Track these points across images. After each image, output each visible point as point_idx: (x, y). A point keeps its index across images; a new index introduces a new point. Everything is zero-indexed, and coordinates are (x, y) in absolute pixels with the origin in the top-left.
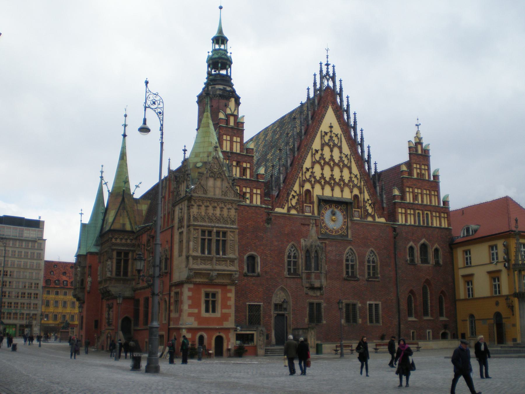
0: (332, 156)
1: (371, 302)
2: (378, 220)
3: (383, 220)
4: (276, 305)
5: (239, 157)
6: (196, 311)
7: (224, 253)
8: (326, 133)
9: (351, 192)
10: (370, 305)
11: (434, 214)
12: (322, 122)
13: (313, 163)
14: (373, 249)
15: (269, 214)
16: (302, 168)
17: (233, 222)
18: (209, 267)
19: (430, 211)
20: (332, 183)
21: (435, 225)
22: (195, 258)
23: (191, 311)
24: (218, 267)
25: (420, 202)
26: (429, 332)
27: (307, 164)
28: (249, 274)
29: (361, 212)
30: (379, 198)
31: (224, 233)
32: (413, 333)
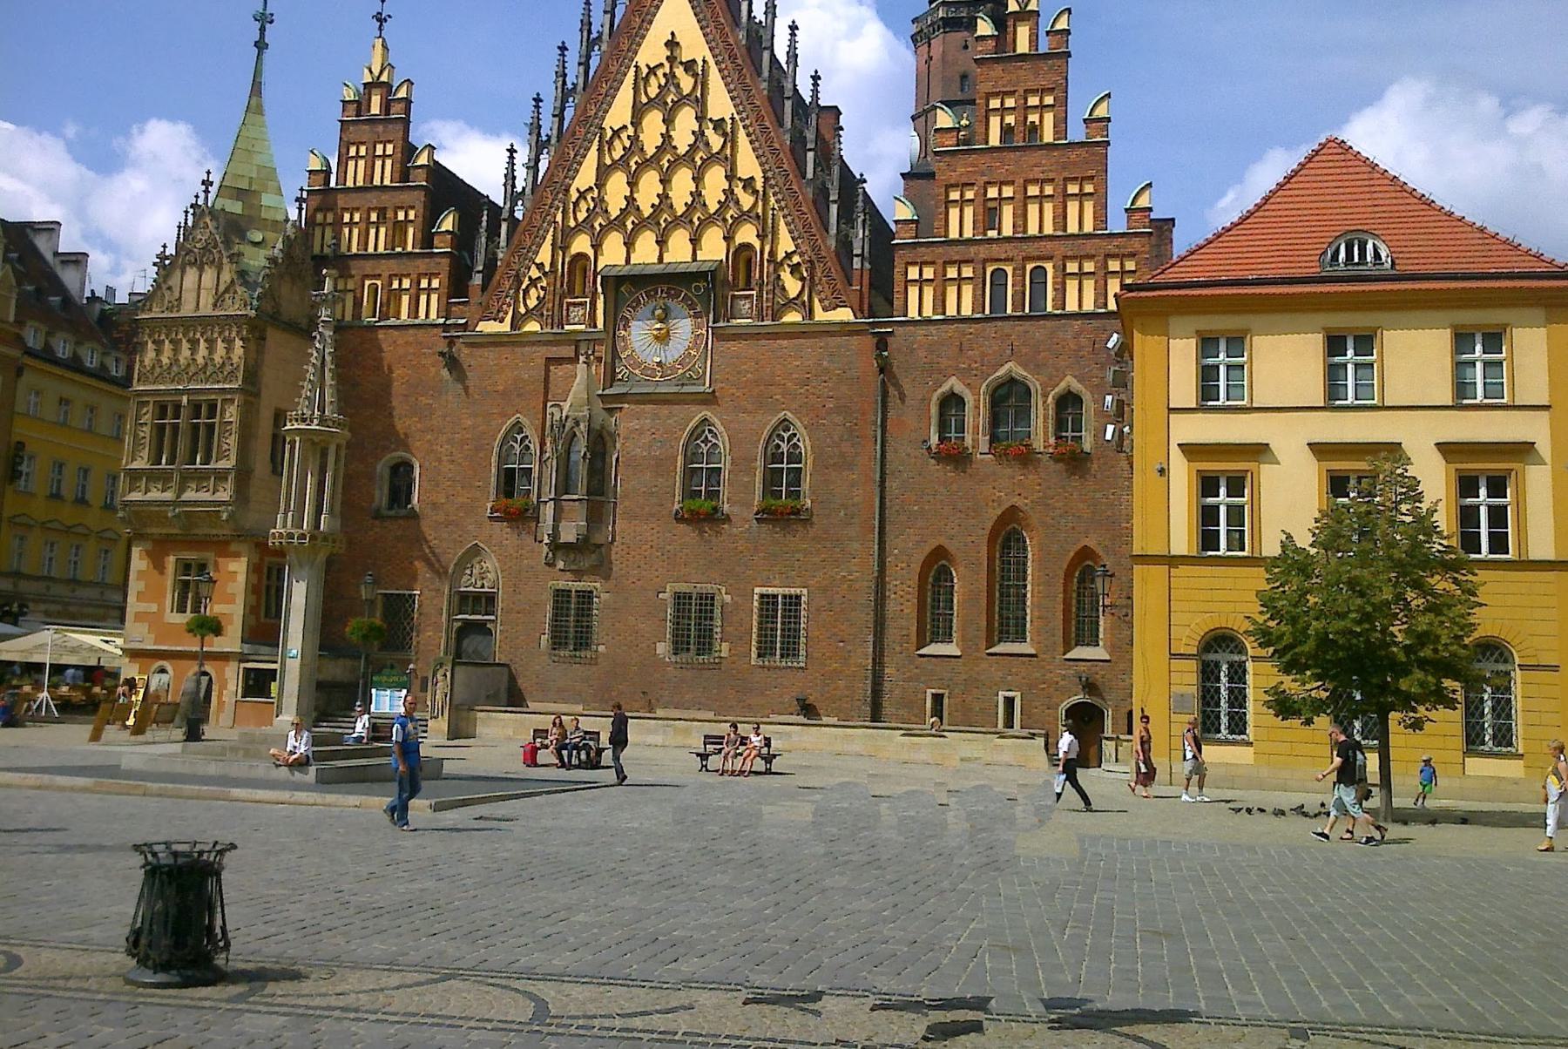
0: (667, 137)
1: (771, 591)
2: (820, 315)
3: (844, 314)
4: (464, 597)
5: (385, 197)
6: (154, 608)
7: (206, 461)
8: (652, 71)
9: (728, 238)
10: (768, 601)
11: (1072, 267)
12: (643, 37)
13: (603, 173)
14: (790, 415)
15: (451, 341)
16: (567, 190)
17: (231, 376)
18: (169, 496)
19: (1050, 258)
20: (662, 221)
21: (1072, 306)
22: (135, 475)
23: (143, 607)
24: (189, 495)
25: (1007, 231)
26: (1009, 702)
27: (585, 177)
28: (385, 512)
29: (760, 296)
30: (832, 243)
31: (212, 407)
32: (938, 698)
